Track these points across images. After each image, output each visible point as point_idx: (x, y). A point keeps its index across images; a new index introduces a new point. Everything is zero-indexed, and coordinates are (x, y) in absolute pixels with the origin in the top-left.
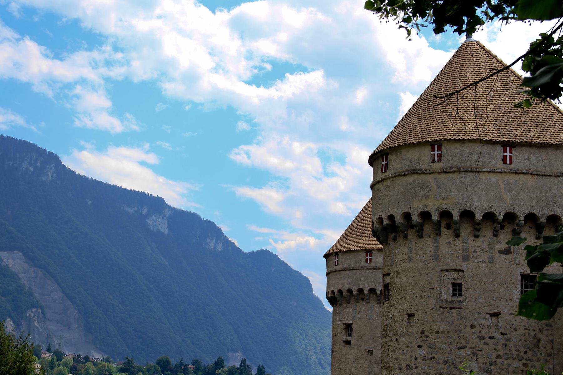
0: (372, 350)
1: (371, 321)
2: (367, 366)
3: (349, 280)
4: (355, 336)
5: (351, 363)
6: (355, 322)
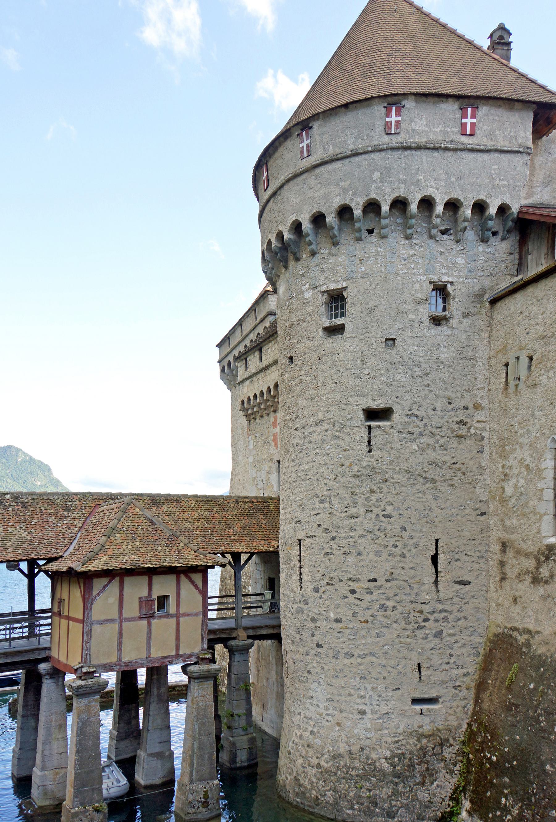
0: (394, 340)
1: (392, 276)
2: (384, 371)
3: (342, 184)
4: (355, 312)
5: (347, 369)
6: (352, 283)
